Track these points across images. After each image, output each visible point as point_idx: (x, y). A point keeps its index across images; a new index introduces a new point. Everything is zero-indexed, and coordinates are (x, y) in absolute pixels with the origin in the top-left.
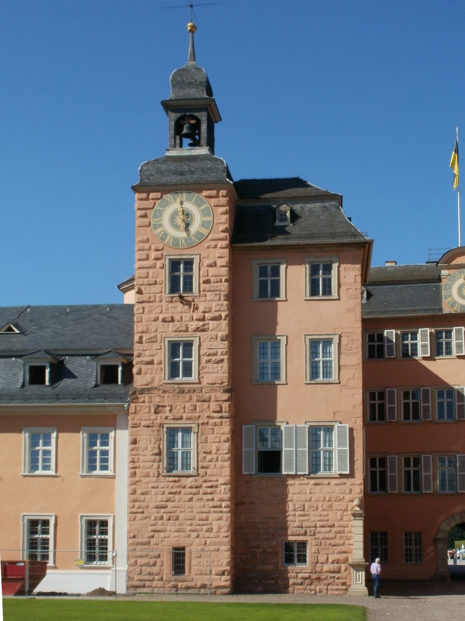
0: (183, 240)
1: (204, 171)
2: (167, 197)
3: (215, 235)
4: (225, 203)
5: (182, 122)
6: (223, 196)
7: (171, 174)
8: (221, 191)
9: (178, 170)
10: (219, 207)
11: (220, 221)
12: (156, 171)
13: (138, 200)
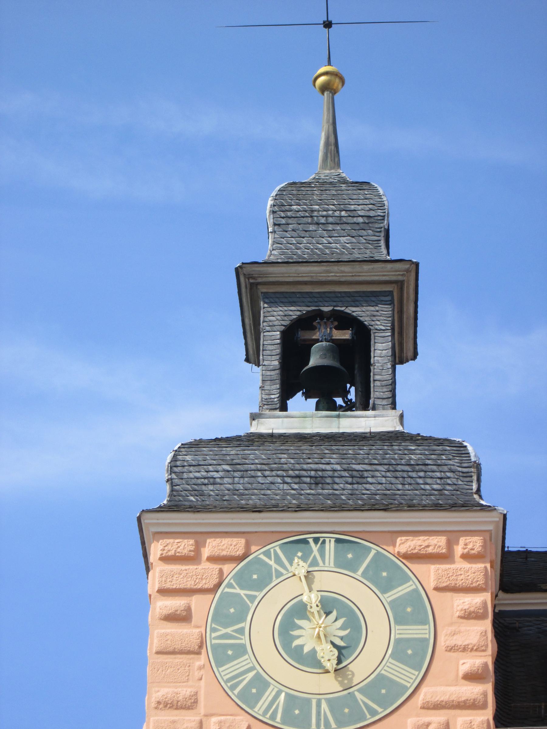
0: (324, 705)
1: (398, 474)
2: (267, 554)
3: (443, 688)
4: (480, 581)
5: (304, 335)
6: (467, 557)
7: (279, 480)
8: (462, 540)
9: (305, 466)
10: (455, 595)
11: (459, 641)
12: (227, 467)
13: (160, 562)
